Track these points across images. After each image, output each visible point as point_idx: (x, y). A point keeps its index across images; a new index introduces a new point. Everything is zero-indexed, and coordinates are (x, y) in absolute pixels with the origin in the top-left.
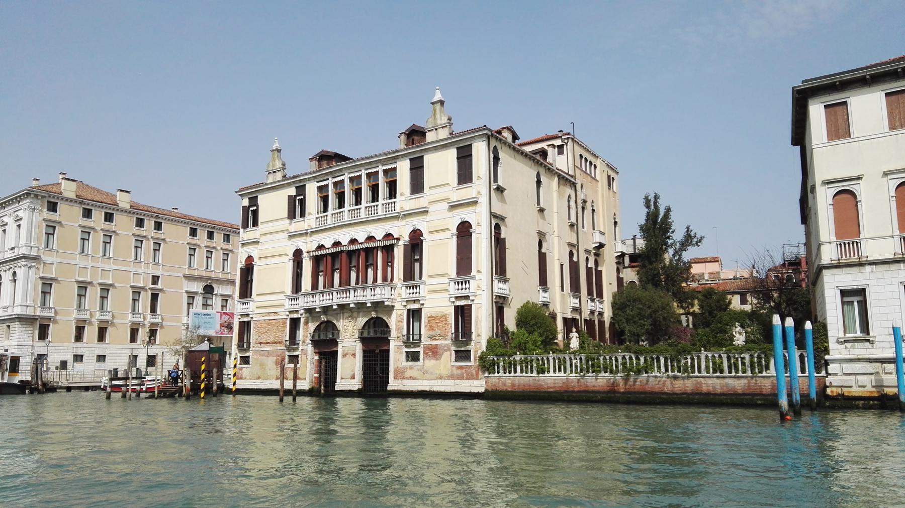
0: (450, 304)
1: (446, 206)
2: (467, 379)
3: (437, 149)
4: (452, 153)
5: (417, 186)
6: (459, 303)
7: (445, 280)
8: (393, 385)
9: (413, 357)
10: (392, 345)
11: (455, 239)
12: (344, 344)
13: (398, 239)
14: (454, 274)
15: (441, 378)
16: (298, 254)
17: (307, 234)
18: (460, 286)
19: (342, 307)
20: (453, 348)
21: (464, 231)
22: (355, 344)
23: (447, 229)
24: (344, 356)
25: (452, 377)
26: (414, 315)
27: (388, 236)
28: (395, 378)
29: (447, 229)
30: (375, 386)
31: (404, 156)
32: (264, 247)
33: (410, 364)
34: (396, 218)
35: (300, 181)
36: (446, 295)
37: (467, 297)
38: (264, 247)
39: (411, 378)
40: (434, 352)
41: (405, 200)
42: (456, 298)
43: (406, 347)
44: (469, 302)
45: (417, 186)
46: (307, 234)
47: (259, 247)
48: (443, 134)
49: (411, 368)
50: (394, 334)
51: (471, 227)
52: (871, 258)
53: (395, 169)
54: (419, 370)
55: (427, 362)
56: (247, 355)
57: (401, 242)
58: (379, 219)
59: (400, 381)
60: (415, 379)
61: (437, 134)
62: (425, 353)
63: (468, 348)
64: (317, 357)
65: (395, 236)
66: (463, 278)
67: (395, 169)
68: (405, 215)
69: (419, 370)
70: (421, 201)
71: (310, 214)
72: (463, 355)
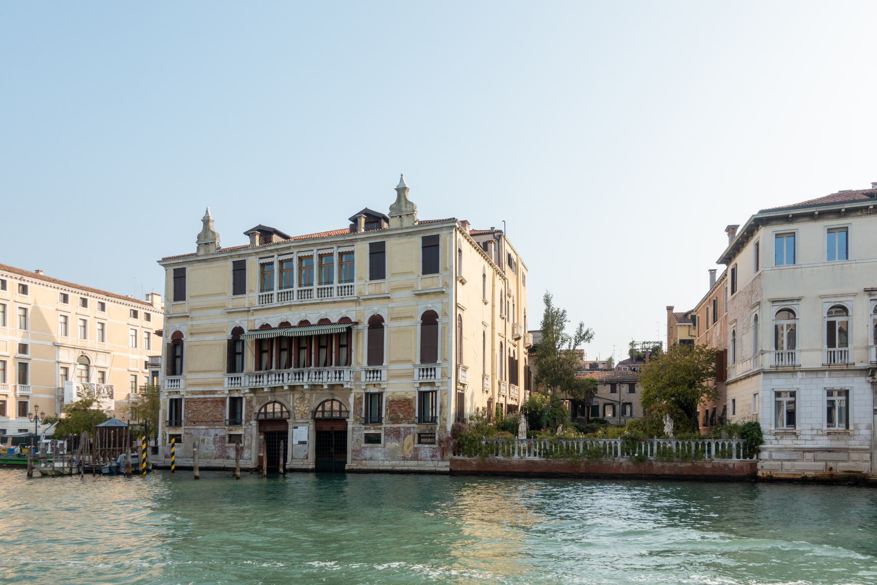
1: (408, 293)
5: (377, 271)
6: (423, 389)
7: (409, 366)
11: (419, 327)
13: (357, 323)
14: (418, 362)
15: (404, 459)
16: (238, 332)
17: (248, 311)
18: (425, 373)
23: (411, 317)
27: (345, 320)
29: (411, 317)
31: (363, 239)
32: (194, 323)
35: (239, 256)
36: (410, 381)
37: (432, 384)
38: (194, 323)
41: (362, 282)
42: (421, 384)
44: (435, 389)
45: (377, 271)
46: (248, 311)
51: (436, 316)
52: (803, 367)
53: (352, 252)
57: (360, 327)
58: (334, 302)
61: (402, 221)
64: (262, 437)
65: (353, 320)
66: (429, 366)
67: (352, 252)
68: (364, 300)
70: (383, 286)
71: (251, 291)
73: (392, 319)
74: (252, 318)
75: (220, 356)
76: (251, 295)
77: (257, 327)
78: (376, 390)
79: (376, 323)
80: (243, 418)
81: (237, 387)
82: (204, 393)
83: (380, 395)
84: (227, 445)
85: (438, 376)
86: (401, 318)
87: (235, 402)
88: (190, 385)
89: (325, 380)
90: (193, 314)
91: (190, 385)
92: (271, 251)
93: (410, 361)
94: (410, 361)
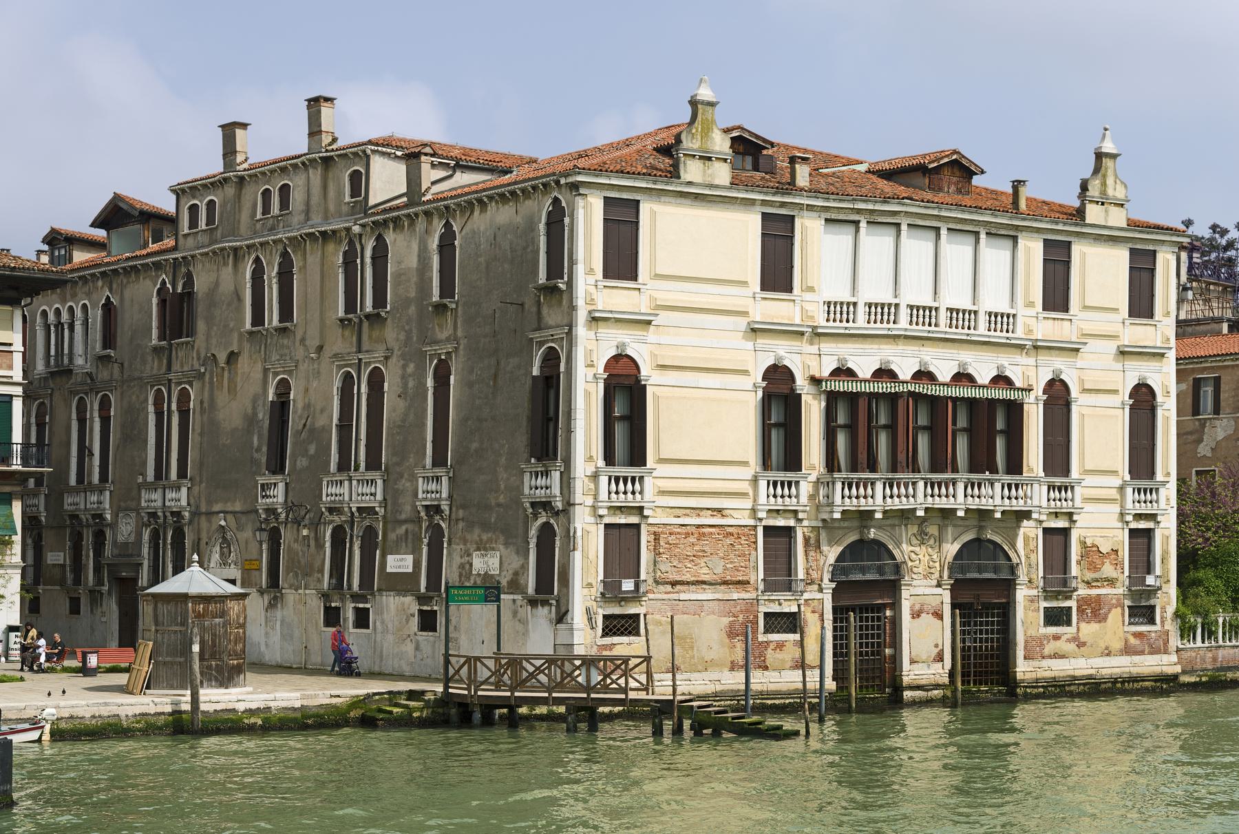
0: (1120, 525)
1: (1112, 346)
2: (1151, 653)
3: (1098, 238)
4: (1120, 258)
8: (1024, 669)
9: (1056, 617)
10: (1022, 594)
12: (913, 591)
16: (778, 376)
19: (905, 516)
20: (1128, 603)
21: (1143, 398)
22: (939, 591)
23: (1115, 392)
24: (916, 615)
25: (1128, 650)
26: (1057, 539)
28: (1025, 658)
30: (985, 673)
33: (1053, 630)
34: (1021, 347)
37: (1152, 517)
38: (665, 339)
39: (1056, 656)
40: (1095, 610)
43: (1046, 599)
47: (652, 335)
48: (1117, 218)
49: (1057, 637)
50: (1022, 577)
54: (1068, 640)
55: (1083, 625)
56: (632, 610)
59: (1036, 663)
60: (1063, 657)
62: (1081, 611)
63: (1152, 602)
65: (1018, 384)
69: (1068, 640)
72: (1143, 612)
73: (1085, 391)
74: (814, 349)
75: (739, 426)
76: (808, 296)
77: (826, 373)
78: (1061, 524)
79: (1058, 397)
80: (801, 575)
81: (791, 503)
82: (698, 510)
83: (1065, 532)
84: (761, 638)
85: (1162, 504)
86: (1098, 391)
87: (779, 538)
88: (663, 493)
89: (998, 501)
90: (663, 318)
91: (663, 493)
92: (859, 211)
93: (1115, 473)
94: (1115, 473)
